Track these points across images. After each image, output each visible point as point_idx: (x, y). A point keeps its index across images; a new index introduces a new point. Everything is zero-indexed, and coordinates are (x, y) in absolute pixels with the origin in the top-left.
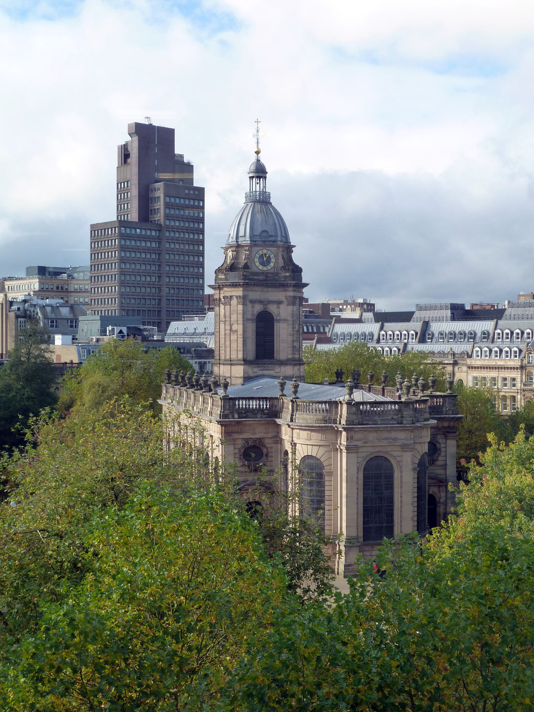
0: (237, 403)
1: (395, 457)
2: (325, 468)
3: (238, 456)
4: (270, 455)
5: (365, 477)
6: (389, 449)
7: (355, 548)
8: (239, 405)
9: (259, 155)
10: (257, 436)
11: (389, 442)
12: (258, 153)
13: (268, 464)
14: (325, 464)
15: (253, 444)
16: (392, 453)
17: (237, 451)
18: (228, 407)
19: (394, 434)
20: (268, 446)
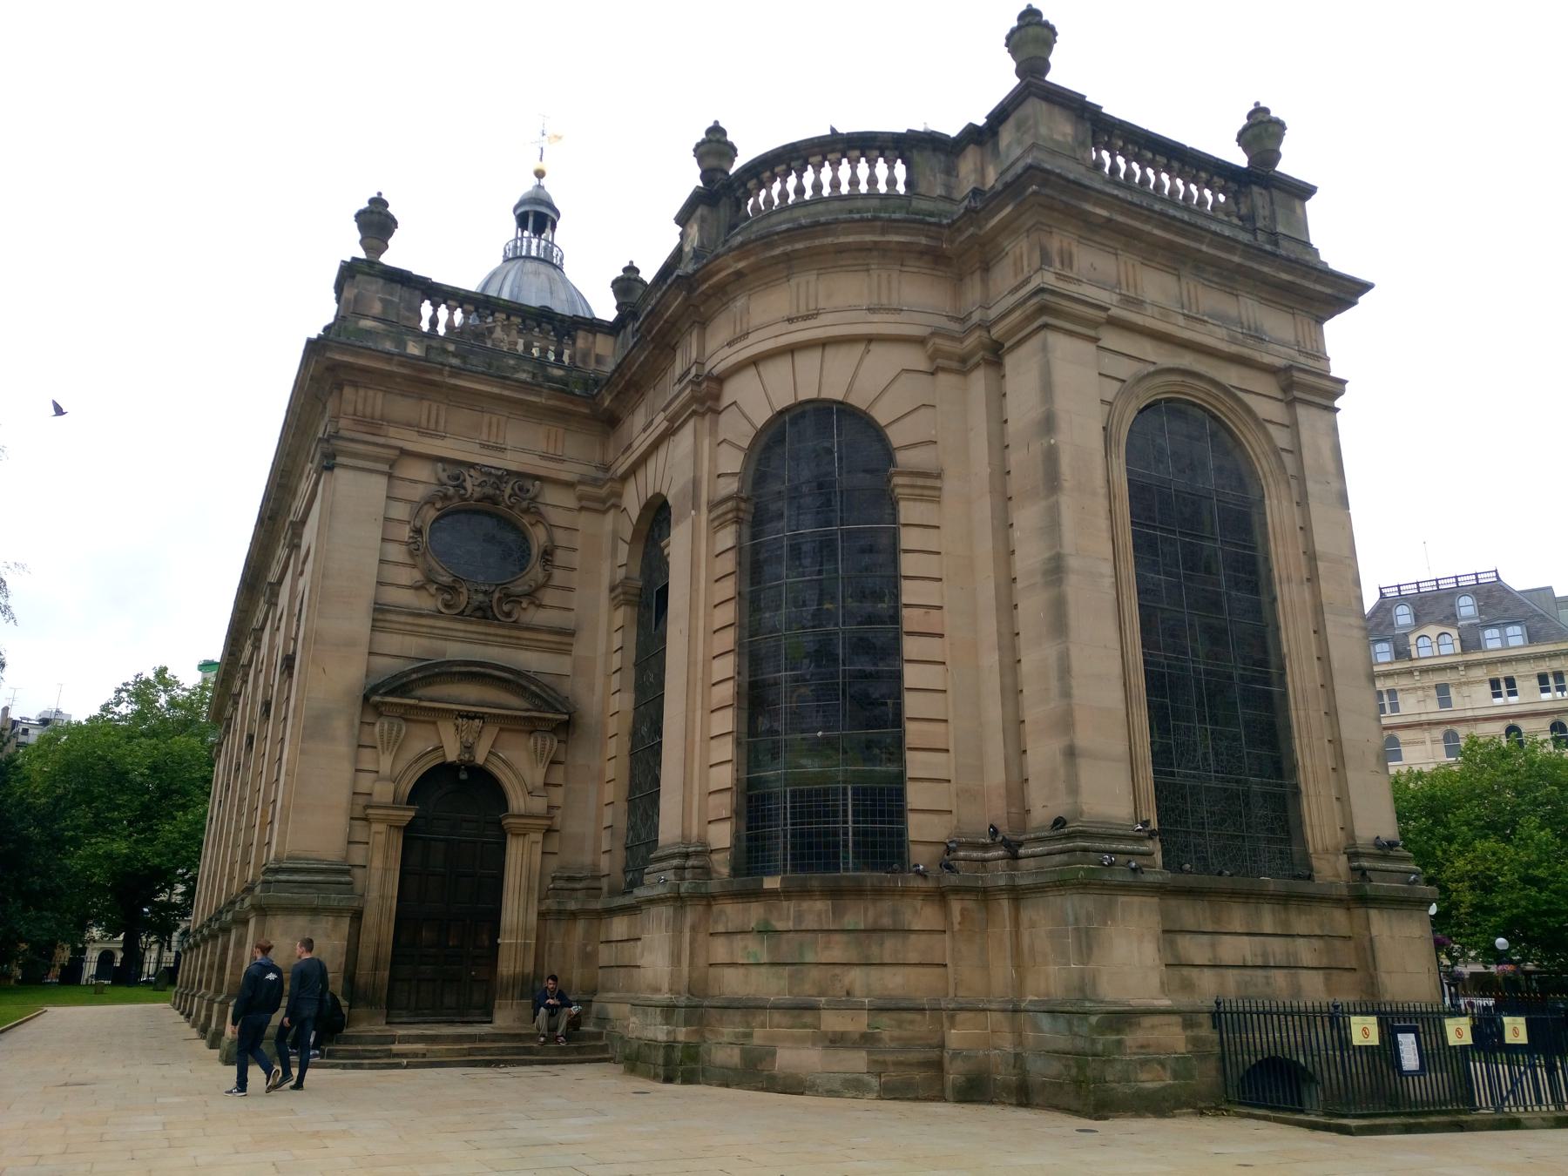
0: (426, 309)
1: (1260, 423)
2: (902, 458)
3: (405, 533)
4: (560, 557)
5: (1138, 490)
6: (1231, 376)
7: (1136, 900)
8: (434, 322)
9: (544, 181)
10: (511, 461)
11: (1233, 341)
12: (540, 174)
13: (549, 597)
14: (896, 437)
15: (489, 491)
16: (1249, 399)
17: (401, 511)
18: (377, 308)
19: (1251, 310)
20: (555, 517)
